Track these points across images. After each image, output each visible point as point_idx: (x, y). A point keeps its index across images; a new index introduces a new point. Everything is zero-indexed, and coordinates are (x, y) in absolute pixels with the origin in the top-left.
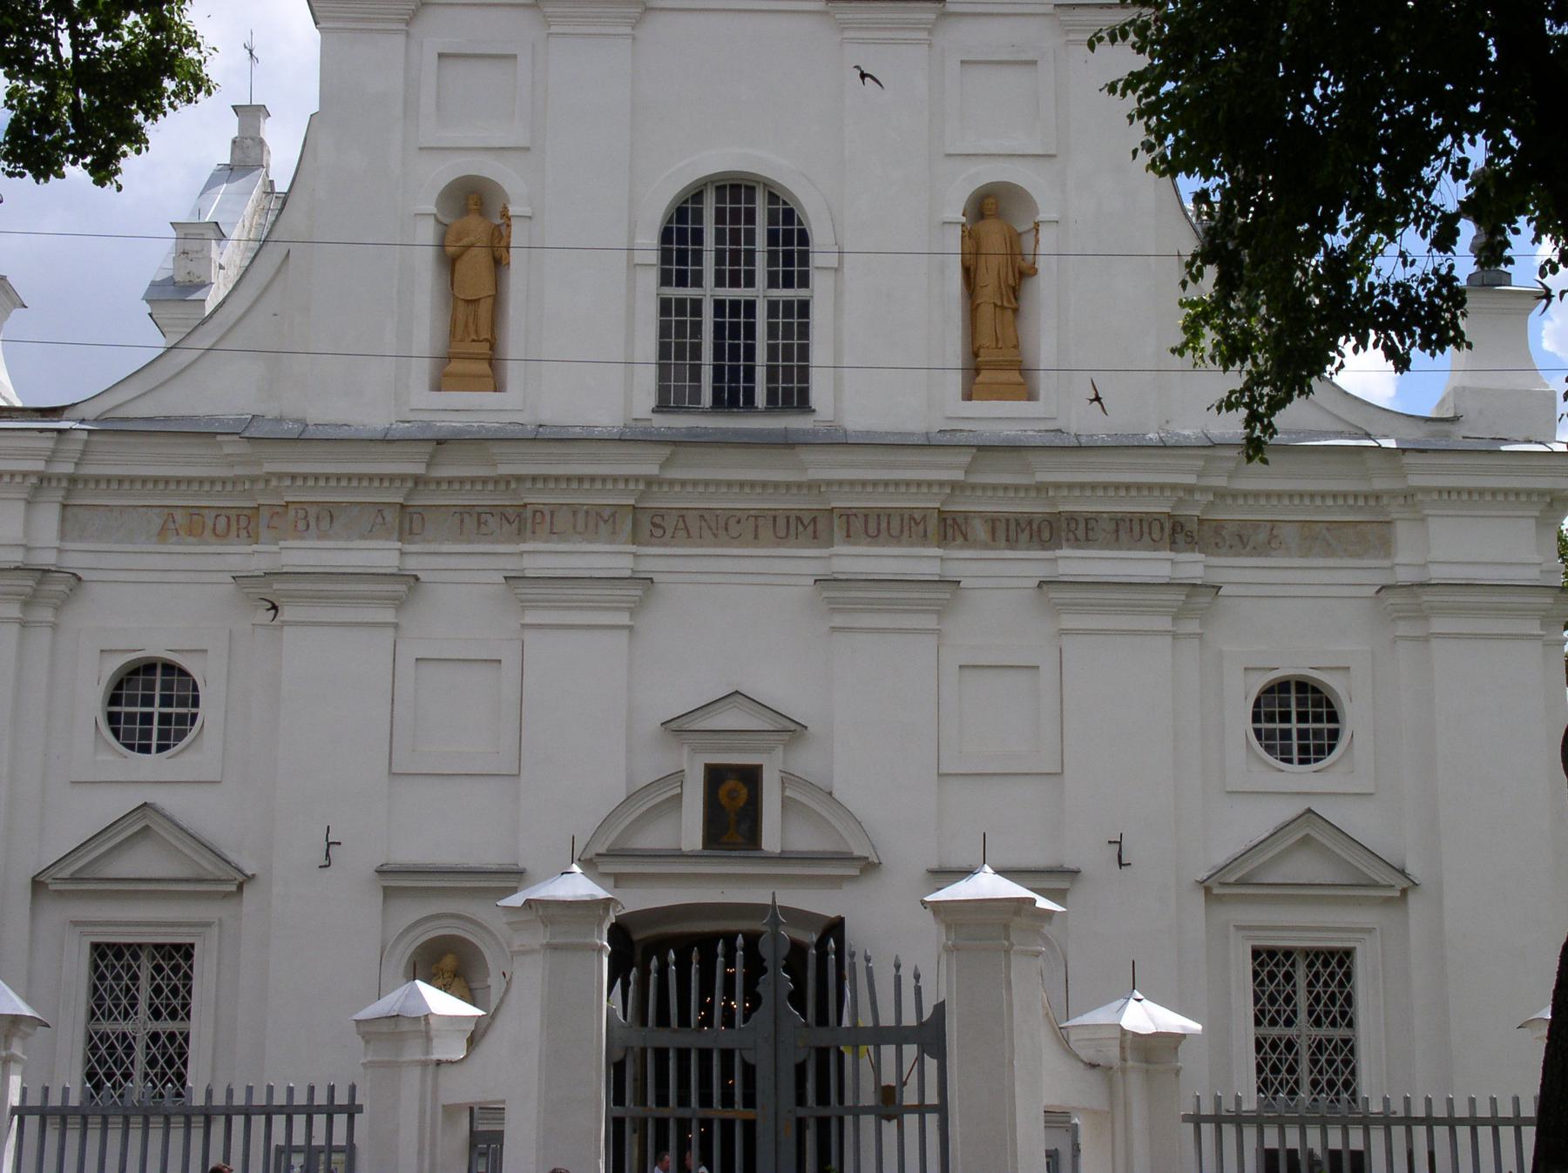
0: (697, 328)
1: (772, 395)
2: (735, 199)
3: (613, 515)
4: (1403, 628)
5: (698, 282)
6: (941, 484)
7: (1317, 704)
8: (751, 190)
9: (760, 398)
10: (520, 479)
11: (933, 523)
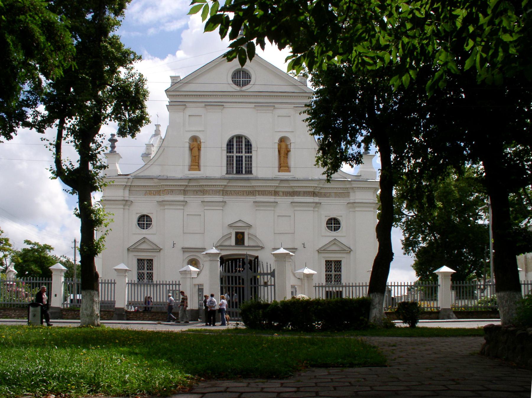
0: (233, 160)
1: (246, 171)
2: (239, 139)
4: (351, 210)
5: (233, 152)
6: (274, 186)
7: (337, 222)
8: (242, 137)
9: (244, 172)
10: (203, 185)
11: (273, 192)
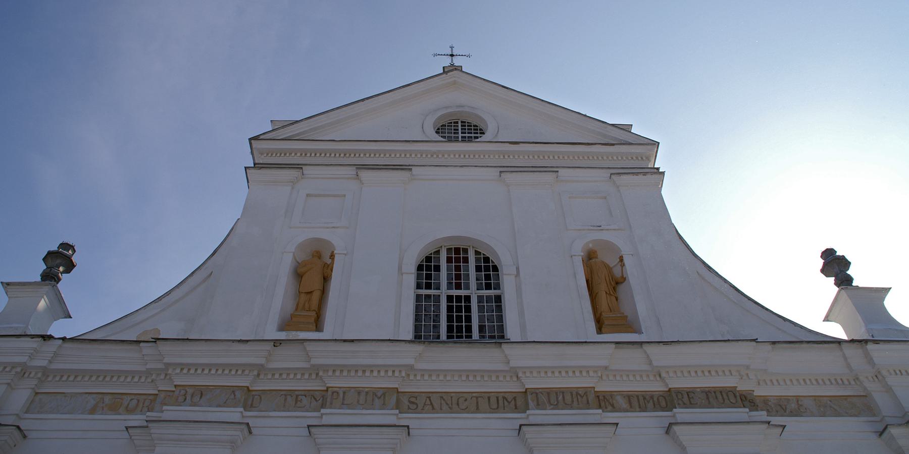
3: (384, 394)
8: (466, 251)
11: (591, 397)
